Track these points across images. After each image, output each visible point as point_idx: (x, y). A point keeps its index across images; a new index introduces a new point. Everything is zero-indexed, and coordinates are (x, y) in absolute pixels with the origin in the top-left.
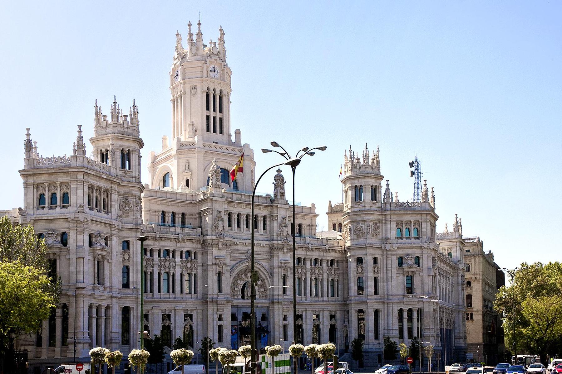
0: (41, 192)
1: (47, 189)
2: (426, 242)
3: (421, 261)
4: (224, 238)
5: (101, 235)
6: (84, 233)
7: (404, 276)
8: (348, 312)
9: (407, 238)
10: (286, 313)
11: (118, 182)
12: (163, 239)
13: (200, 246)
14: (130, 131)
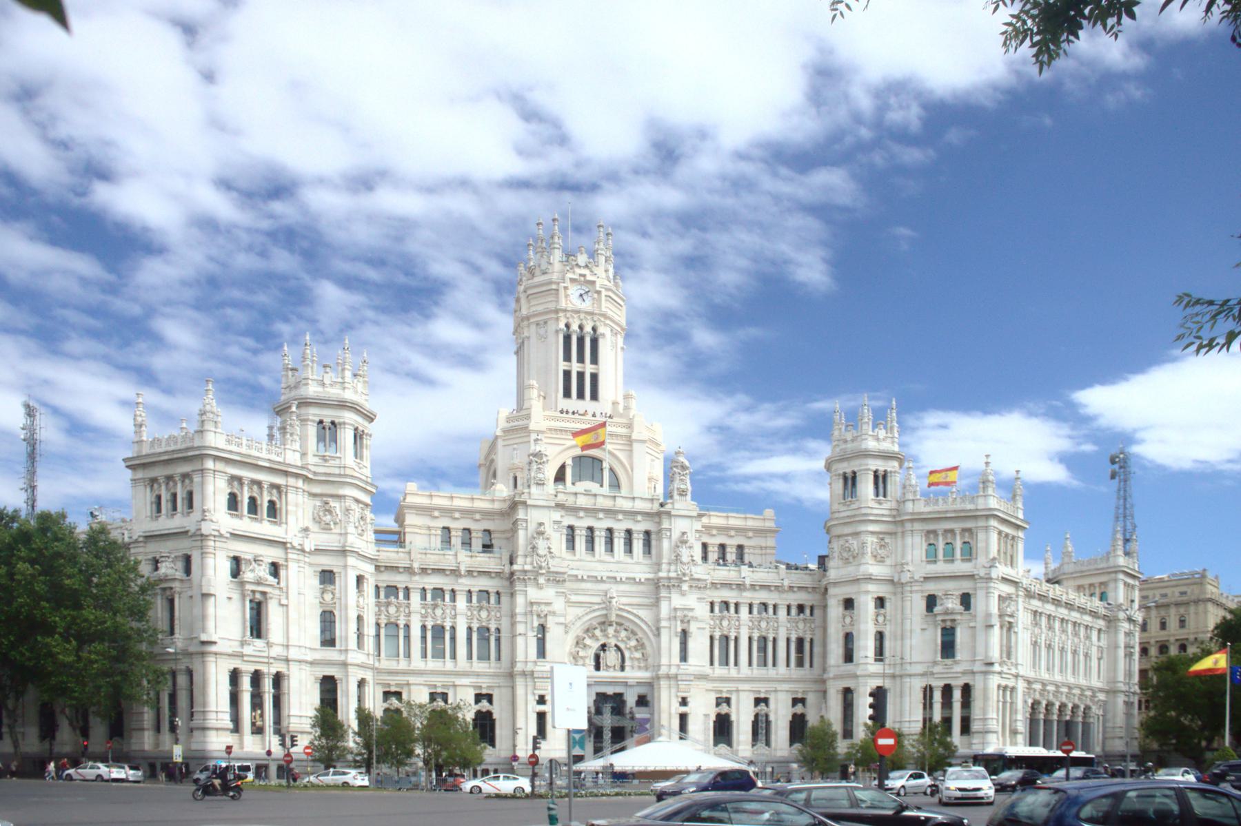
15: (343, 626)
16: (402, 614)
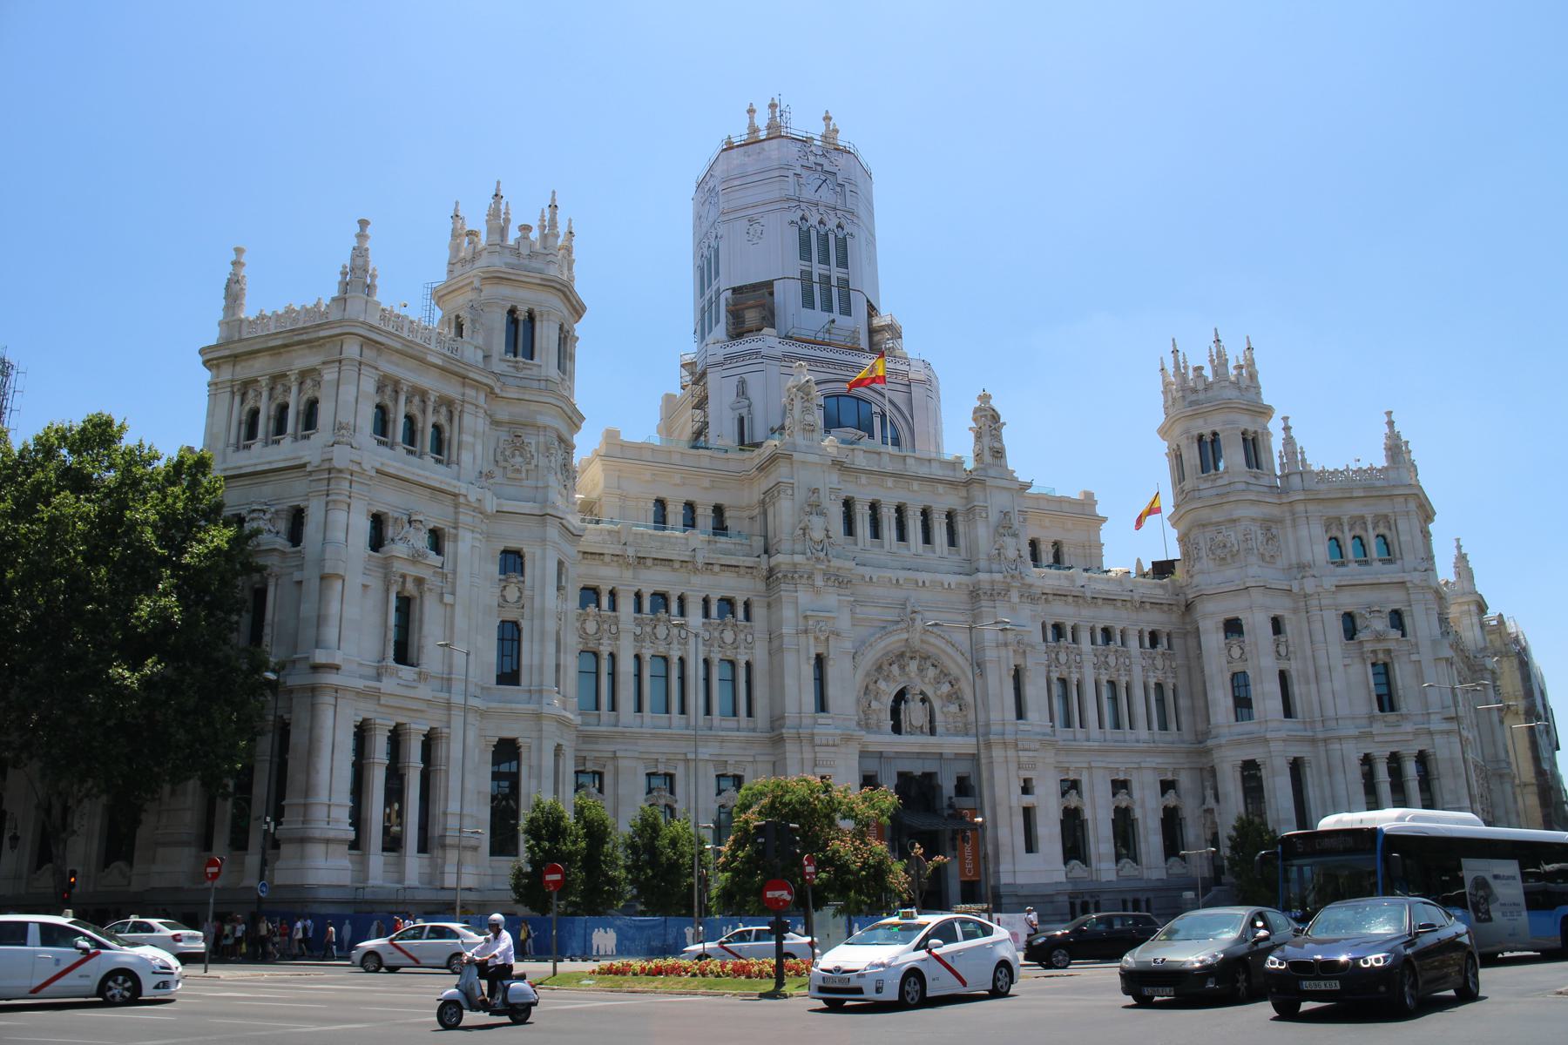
2: (1415, 570)
3: (1407, 621)
4: (829, 561)
5: (414, 518)
6: (349, 505)
7: (1365, 664)
8: (1213, 772)
9: (1360, 563)
10: (1028, 775)
11: (486, 385)
12: (649, 562)
13: (761, 586)
14: (536, 264)
15: (536, 647)
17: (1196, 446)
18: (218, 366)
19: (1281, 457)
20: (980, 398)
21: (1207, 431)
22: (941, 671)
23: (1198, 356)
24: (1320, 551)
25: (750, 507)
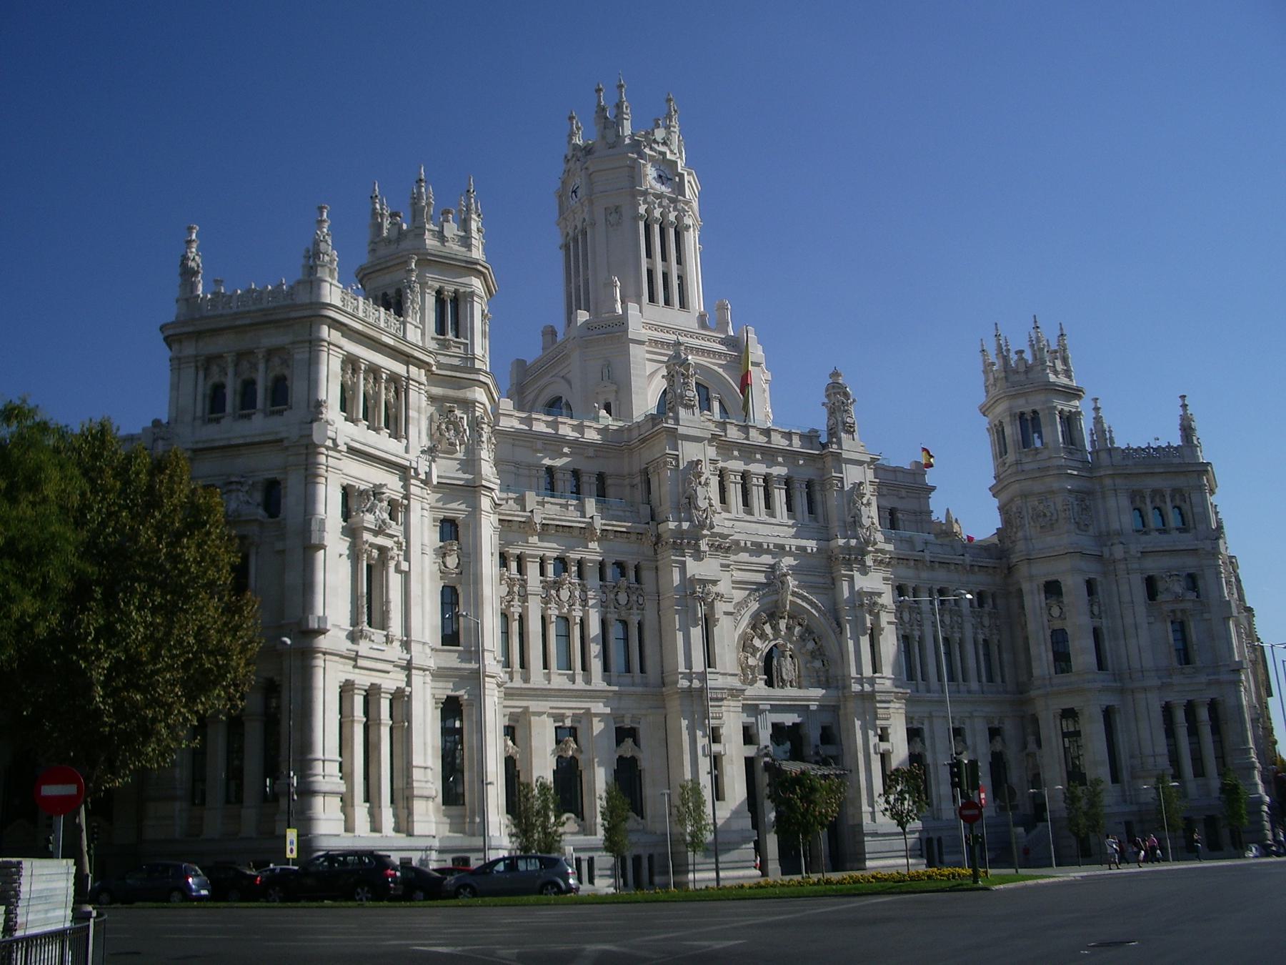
0: (216, 378)
1: (230, 371)
3: (1201, 584)
6: (326, 479)
8: (1035, 720)
16: (517, 597)
17: (1018, 422)
18: (180, 342)
19: (1092, 434)
20: (832, 375)
21: (1027, 409)
22: (807, 630)
23: (1018, 341)
24: (1128, 520)
25: (631, 475)
